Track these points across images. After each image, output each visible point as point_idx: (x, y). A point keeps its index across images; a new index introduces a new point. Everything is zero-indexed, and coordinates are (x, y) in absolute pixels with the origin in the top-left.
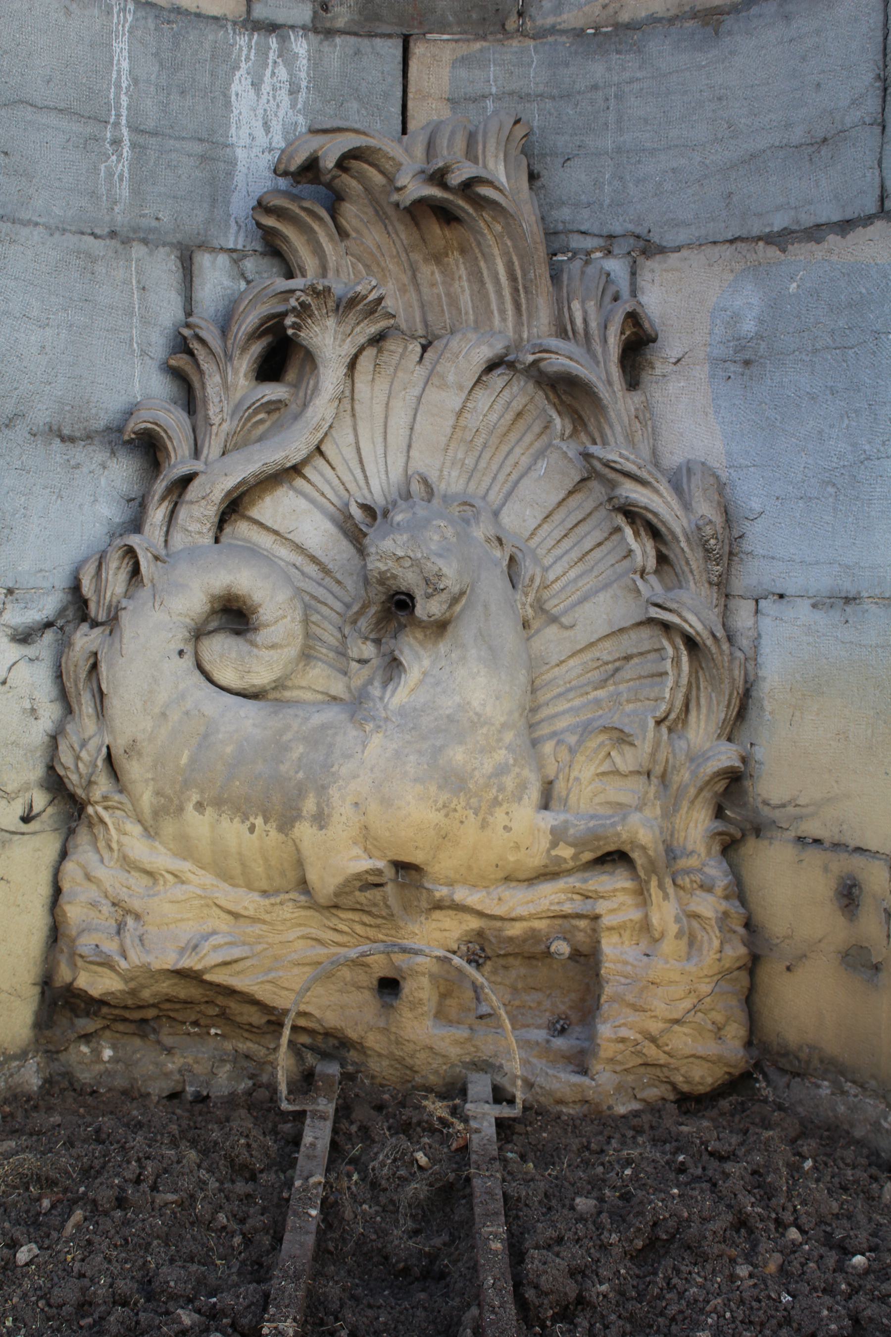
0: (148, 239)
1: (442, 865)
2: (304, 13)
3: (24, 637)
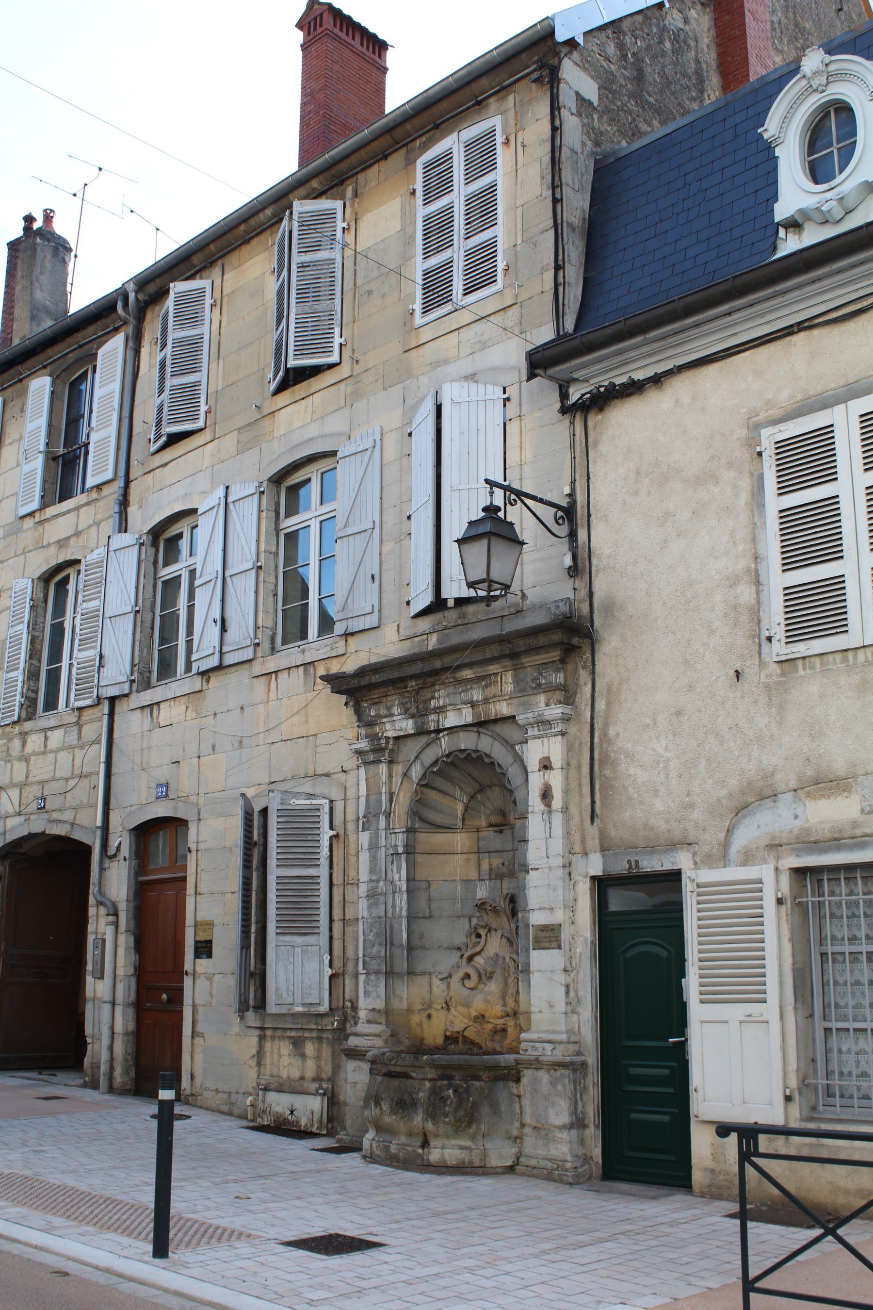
0: (463, 916)
1: (487, 1015)
2: (487, 877)
3: (441, 980)
